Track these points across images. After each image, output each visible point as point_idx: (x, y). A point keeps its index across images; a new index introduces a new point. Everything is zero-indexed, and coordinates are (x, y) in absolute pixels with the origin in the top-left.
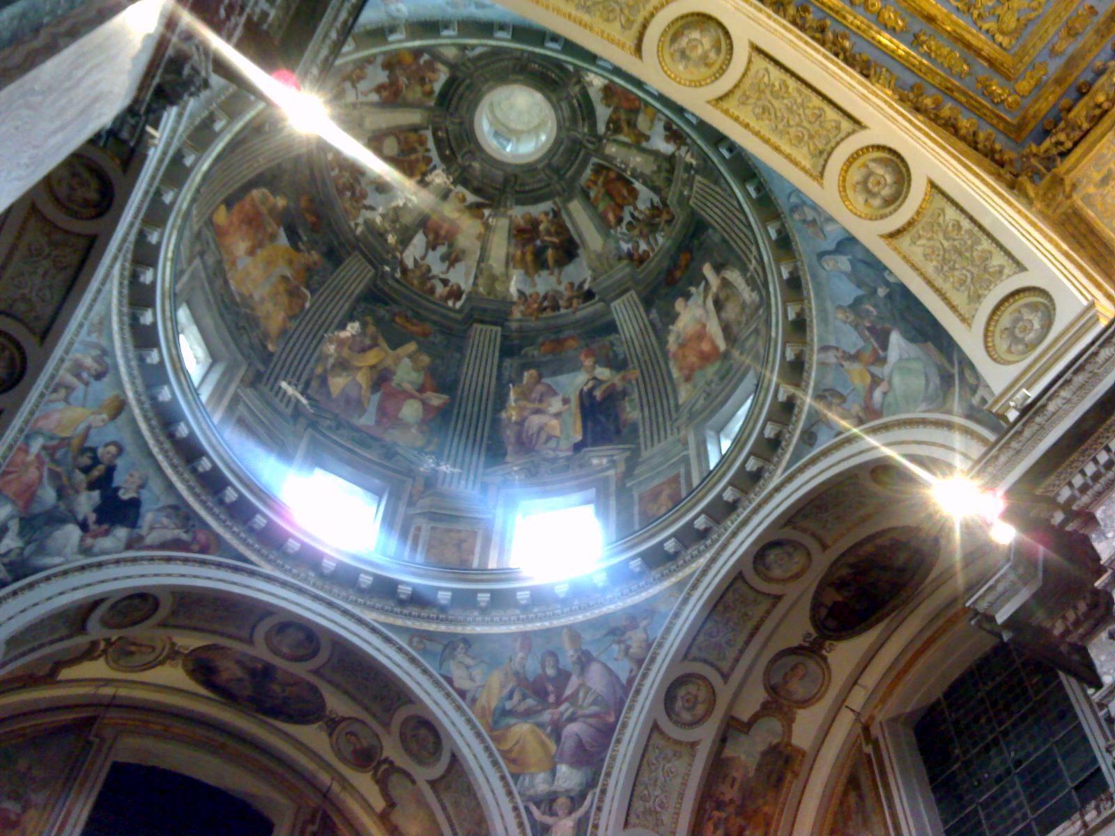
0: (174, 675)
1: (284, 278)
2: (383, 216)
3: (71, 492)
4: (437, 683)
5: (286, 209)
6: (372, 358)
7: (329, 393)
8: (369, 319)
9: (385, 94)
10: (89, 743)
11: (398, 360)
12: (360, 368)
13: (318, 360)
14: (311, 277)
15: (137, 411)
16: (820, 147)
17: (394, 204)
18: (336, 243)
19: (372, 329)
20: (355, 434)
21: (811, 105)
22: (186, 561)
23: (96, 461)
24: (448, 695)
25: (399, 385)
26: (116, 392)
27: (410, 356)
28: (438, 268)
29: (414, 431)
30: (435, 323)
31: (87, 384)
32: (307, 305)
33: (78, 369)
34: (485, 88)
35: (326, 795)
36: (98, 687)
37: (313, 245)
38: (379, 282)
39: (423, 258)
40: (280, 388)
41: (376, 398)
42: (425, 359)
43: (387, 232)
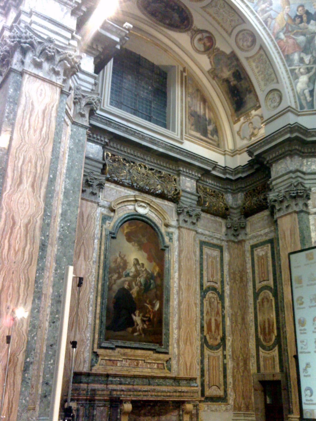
3: (305, 31)
23: (301, 17)
31: (271, 9)
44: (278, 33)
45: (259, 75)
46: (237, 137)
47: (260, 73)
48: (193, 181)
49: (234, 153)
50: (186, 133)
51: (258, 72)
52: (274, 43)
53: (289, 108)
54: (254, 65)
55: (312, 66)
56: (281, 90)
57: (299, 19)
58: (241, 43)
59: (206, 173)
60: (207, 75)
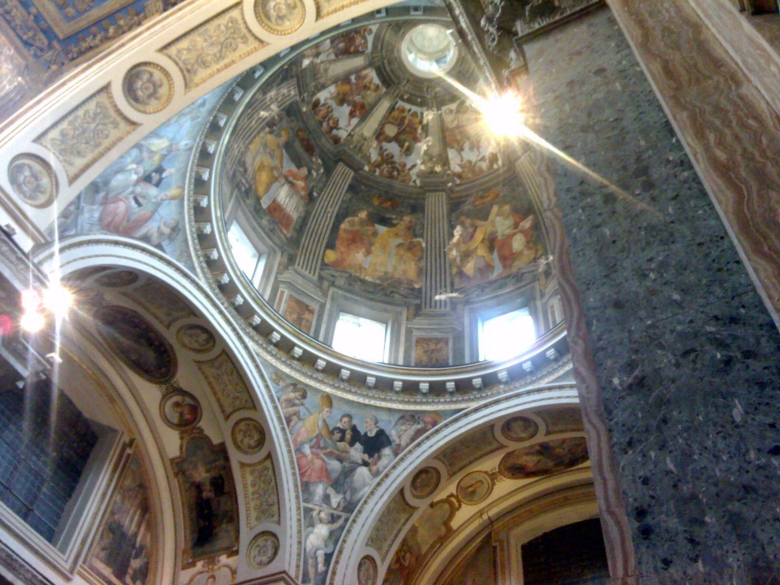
0: (505, 485)
1: (399, 246)
2: (423, 163)
3: (344, 455)
5: (370, 215)
6: (479, 236)
7: (468, 277)
8: (463, 218)
9: (358, 113)
10: (495, 547)
11: (493, 224)
12: (477, 248)
13: (450, 266)
14: (414, 230)
15: (340, 394)
17: (422, 152)
18: (412, 201)
19: (468, 222)
20: (495, 285)
22: (428, 438)
23: (343, 432)
26: (319, 396)
27: (498, 215)
29: (526, 252)
31: (302, 404)
32: (424, 245)
33: (291, 403)
34: (396, 54)
36: (481, 516)
37: (401, 215)
38: (453, 196)
39: (462, 160)
40: (436, 301)
41: (495, 255)
42: (507, 208)
43: (433, 168)
44: (302, 443)
47: (256, 496)
50: (84, 562)
51: (253, 494)
52: (291, 457)
53: (284, 575)
54: (250, 479)
57: (340, 435)
58: (239, 437)
60: (168, 463)
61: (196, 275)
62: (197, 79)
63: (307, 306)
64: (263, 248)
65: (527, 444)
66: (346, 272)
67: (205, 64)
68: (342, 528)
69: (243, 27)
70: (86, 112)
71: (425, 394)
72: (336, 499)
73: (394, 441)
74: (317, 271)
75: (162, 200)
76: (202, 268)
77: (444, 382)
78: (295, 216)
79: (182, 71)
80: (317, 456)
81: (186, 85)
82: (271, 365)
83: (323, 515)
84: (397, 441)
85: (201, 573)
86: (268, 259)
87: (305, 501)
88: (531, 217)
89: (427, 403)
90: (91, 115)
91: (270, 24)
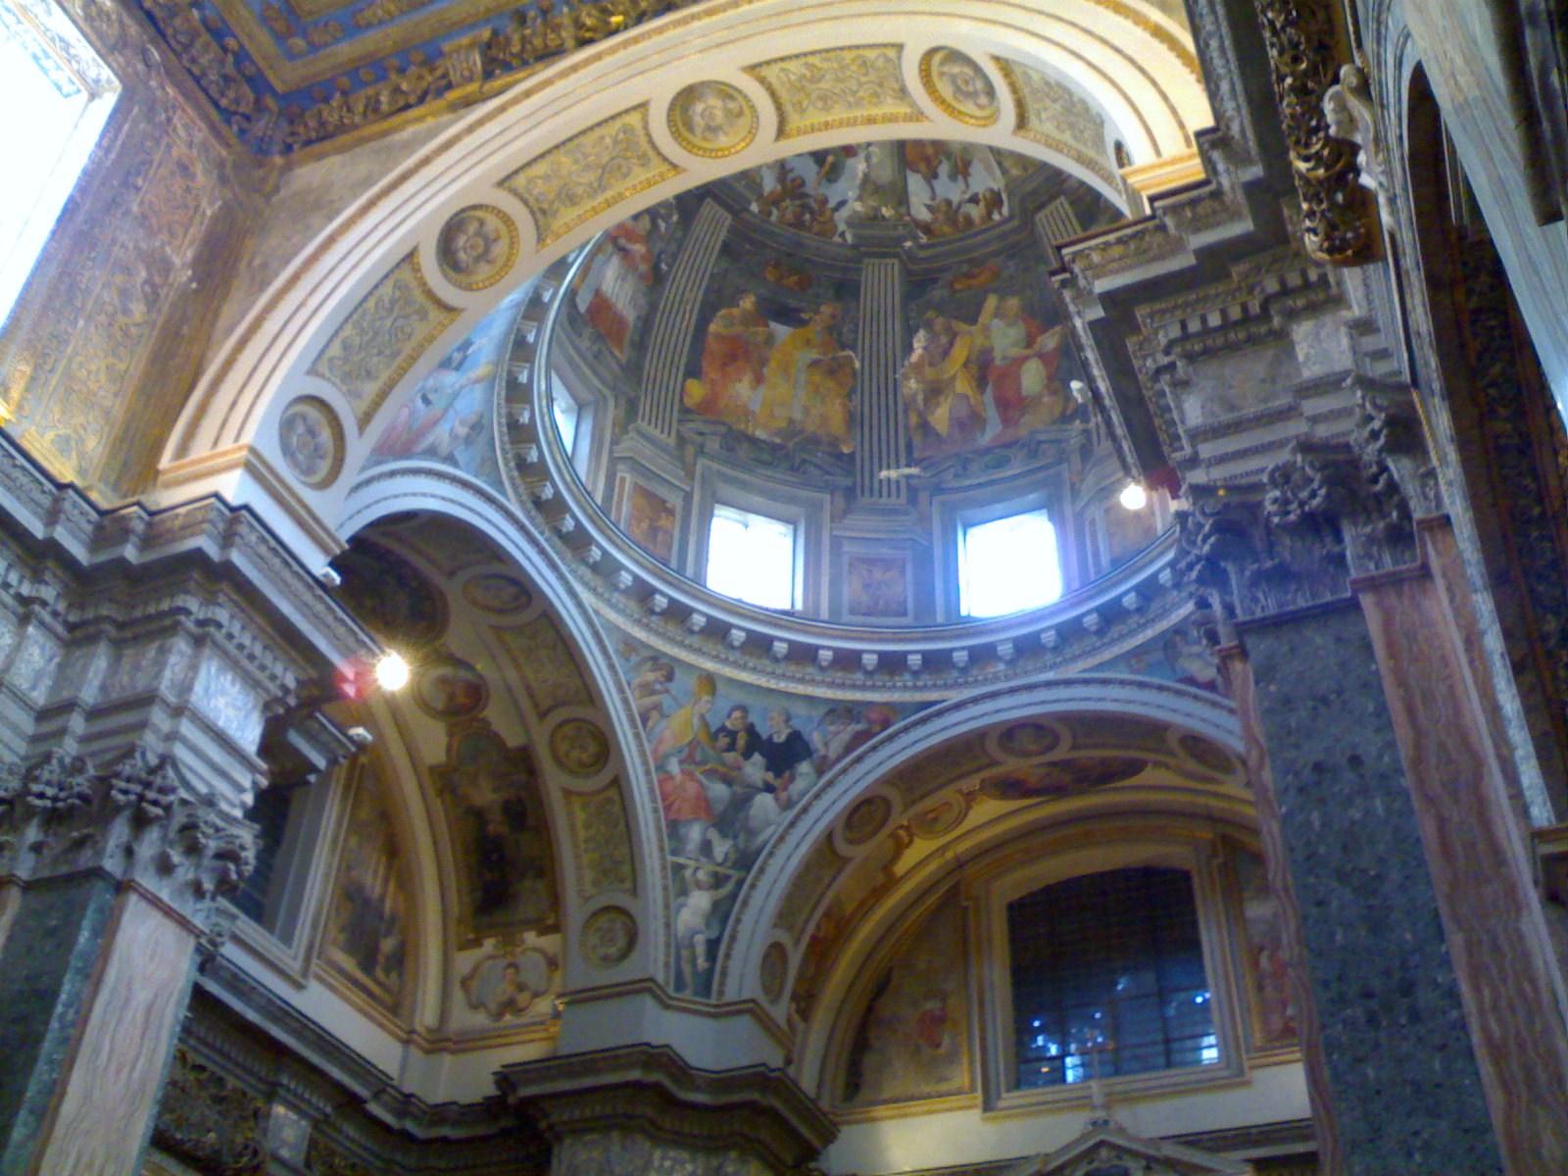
1: (815, 363)
2: (860, 198)
3: (735, 774)
4: (1179, 693)
5: (761, 302)
6: (960, 353)
7: (938, 435)
8: (930, 314)
10: (966, 908)
11: (986, 329)
12: (953, 378)
13: (906, 411)
14: (840, 334)
15: (728, 671)
16: (896, 86)
18: (837, 275)
19: (940, 323)
20: (988, 458)
21: (848, 61)
22: (874, 748)
23: (733, 735)
24: (1196, 697)
25: (1004, 358)
27: (996, 315)
28: (954, 192)
30: (997, 254)
31: (667, 691)
32: (857, 365)
33: (647, 689)
35: (1210, 818)
36: (943, 854)
39: (933, 198)
40: (881, 481)
42: (1013, 303)
43: (877, 209)
44: (667, 756)
45: (586, 851)
46: (458, 995)
48: (304, 1123)
49: (440, 1042)
51: (586, 841)
55: (731, 872)
56: (639, 920)
58: (563, 747)
59: (351, 1103)
61: (503, 493)
62: (557, 224)
63: (664, 502)
64: (585, 395)
65: (1037, 760)
66: (723, 424)
67: (572, 200)
68: (734, 896)
69: (643, 140)
70: (380, 300)
71: (869, 674)
72: (721, 848)
73: (816, 750)
74: (675, 426)
75: (462, 387)
76: (511, 479)
77: (906, 654)
78: (630, 316)
79: (532, 212)
80: (690, 775)
81: (541, 239)
82: (618, 628)
83: (701, 875)
84: (822, 752)
85: (491, 957)
86: (595, 417)
87: (674, 853)
88: (1058, 328)
89: (874, 688)
90: (387, 305)
91: (690, 137)
